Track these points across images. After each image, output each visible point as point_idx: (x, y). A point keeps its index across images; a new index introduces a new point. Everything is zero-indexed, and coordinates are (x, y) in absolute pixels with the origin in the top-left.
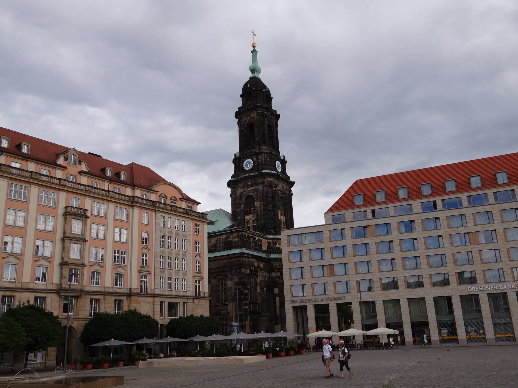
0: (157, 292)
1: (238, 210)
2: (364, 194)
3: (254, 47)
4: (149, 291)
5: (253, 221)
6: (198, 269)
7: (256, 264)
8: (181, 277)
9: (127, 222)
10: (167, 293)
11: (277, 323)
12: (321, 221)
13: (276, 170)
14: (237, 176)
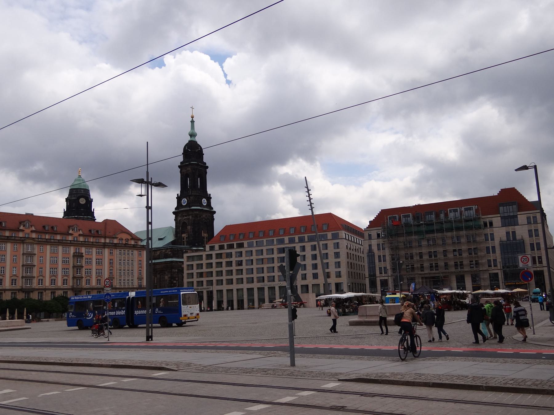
0: (118, 287)
3: (192, 117)
4: (114, 287)
6: (140, 274)
8: (130, 279)
10: (123, 287)
13: (201, 205)
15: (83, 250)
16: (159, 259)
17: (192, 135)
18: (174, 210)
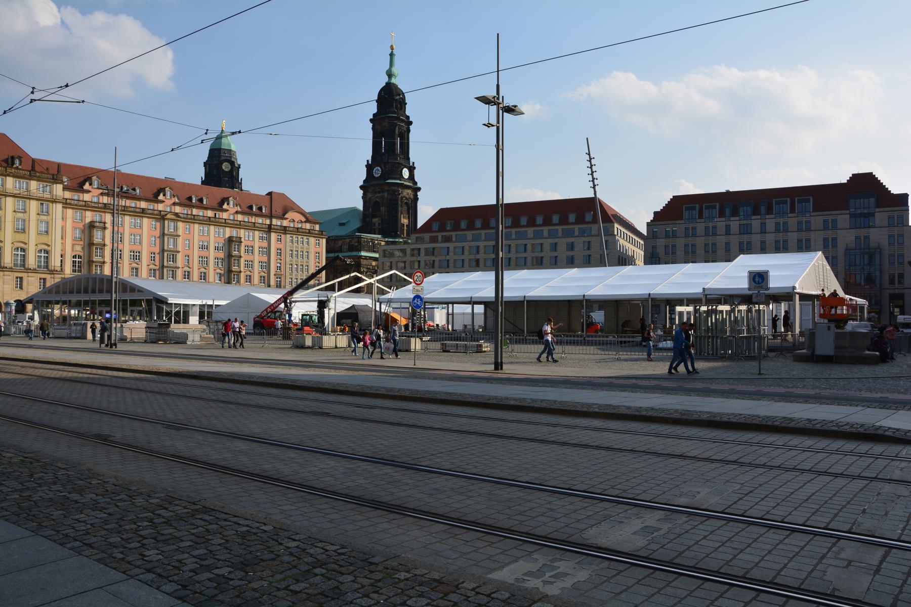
16: (341, 251)
17: (390, 75)
18: (362, 183)
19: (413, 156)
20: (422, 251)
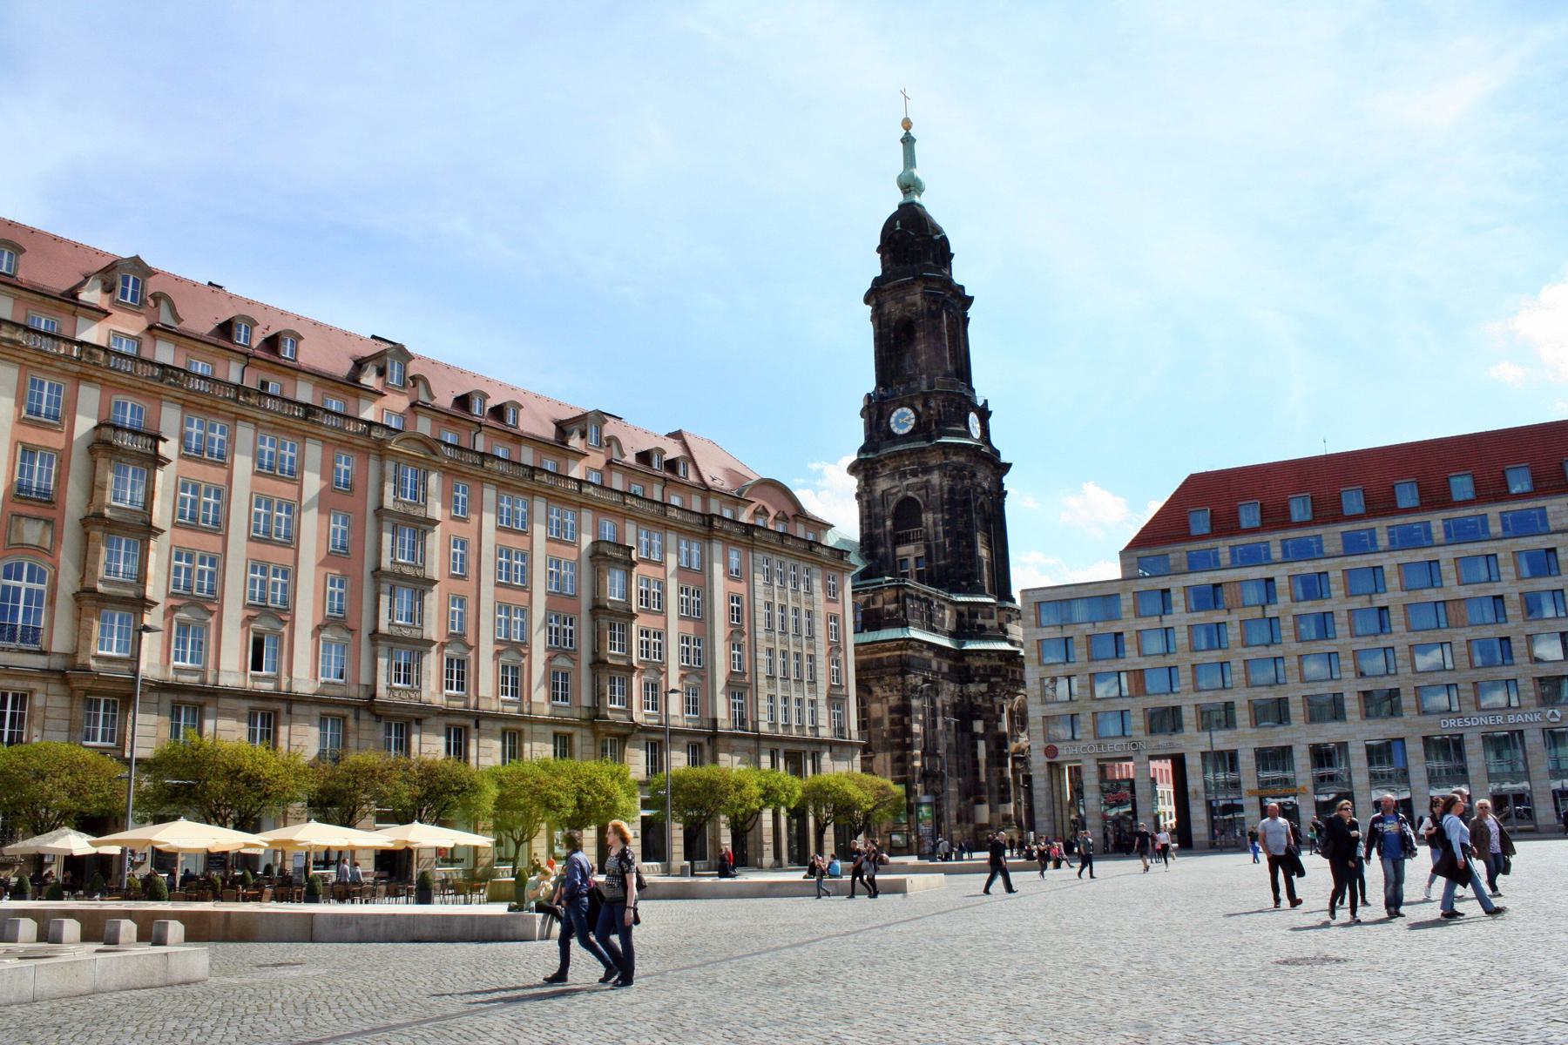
1: (880, 531)
2: (1212, 513)
3: (907, 124)
5: (917, 559)
7: (934, 665)
9: (702, 571)
11: (980, 802)
12: (1111, 570)
13: (968, 435)
14: (876, 450)
15: (631, 535)
17: (910, 186)
19: (984, 385)
20: (1177, 598)
